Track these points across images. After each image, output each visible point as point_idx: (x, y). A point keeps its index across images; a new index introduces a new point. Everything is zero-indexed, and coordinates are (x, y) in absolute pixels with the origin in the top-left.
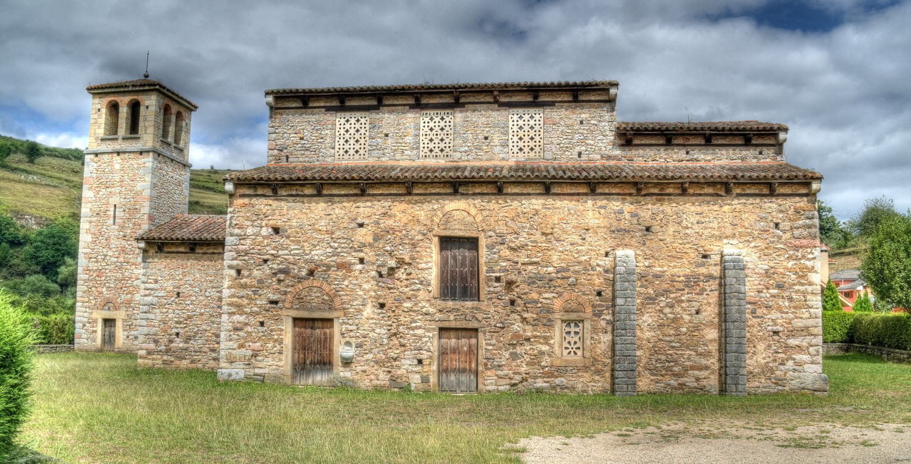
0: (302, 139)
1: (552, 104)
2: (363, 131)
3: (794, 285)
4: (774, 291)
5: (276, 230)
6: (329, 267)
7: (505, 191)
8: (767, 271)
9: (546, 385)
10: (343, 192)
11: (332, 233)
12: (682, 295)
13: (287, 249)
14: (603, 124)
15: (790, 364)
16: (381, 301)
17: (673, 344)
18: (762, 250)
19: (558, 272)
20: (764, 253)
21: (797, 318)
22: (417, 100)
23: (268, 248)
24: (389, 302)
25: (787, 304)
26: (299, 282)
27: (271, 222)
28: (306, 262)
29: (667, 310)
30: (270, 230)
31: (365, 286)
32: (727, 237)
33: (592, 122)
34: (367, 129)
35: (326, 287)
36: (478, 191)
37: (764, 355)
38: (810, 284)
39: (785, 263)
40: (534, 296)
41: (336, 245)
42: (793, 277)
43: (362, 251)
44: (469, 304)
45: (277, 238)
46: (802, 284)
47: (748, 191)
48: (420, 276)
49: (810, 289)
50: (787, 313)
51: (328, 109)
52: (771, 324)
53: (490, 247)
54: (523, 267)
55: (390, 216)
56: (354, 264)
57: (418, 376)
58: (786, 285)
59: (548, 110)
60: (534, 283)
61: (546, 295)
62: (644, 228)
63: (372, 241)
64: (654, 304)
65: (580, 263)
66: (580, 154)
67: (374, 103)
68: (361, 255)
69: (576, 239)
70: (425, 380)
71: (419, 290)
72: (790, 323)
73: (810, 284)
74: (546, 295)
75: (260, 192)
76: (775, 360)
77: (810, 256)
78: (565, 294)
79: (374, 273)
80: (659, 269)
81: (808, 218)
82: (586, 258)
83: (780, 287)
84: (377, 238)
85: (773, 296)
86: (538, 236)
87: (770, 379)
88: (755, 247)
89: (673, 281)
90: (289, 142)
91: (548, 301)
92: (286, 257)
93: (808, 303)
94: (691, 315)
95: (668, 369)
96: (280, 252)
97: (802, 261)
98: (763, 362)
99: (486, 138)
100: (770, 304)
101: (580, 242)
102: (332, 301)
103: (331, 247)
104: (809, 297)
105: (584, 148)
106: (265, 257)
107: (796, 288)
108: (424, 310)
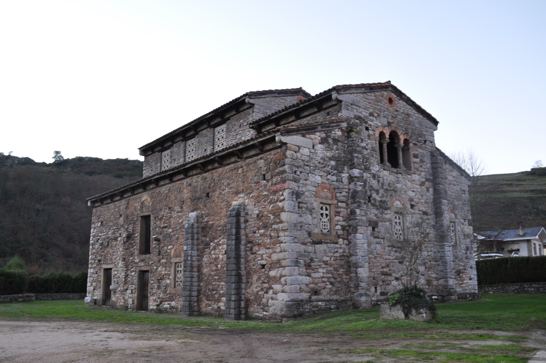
1: (229, 119)
3: (273, 224)
4: (262, 231)
12: (220, 241)
15: (271, 292)
20: (258, 200)
21: (275, 252)
22: (184, 137)
25: (269, 241)
38: (281, 222)
42: (272, 217)
49: (281, 225)
69: (179, 210)
72: (270, 257)
73: (281, 222)
76: (262, 289)
77: (282, 198)
80: (211, 223)
81: (281, 166)
83: (265, 227)
88: (252, 197)
89: (217, 230)
94: (222, 254)
100: (260, 242)
104: (281, 234)
107: (273, 226)
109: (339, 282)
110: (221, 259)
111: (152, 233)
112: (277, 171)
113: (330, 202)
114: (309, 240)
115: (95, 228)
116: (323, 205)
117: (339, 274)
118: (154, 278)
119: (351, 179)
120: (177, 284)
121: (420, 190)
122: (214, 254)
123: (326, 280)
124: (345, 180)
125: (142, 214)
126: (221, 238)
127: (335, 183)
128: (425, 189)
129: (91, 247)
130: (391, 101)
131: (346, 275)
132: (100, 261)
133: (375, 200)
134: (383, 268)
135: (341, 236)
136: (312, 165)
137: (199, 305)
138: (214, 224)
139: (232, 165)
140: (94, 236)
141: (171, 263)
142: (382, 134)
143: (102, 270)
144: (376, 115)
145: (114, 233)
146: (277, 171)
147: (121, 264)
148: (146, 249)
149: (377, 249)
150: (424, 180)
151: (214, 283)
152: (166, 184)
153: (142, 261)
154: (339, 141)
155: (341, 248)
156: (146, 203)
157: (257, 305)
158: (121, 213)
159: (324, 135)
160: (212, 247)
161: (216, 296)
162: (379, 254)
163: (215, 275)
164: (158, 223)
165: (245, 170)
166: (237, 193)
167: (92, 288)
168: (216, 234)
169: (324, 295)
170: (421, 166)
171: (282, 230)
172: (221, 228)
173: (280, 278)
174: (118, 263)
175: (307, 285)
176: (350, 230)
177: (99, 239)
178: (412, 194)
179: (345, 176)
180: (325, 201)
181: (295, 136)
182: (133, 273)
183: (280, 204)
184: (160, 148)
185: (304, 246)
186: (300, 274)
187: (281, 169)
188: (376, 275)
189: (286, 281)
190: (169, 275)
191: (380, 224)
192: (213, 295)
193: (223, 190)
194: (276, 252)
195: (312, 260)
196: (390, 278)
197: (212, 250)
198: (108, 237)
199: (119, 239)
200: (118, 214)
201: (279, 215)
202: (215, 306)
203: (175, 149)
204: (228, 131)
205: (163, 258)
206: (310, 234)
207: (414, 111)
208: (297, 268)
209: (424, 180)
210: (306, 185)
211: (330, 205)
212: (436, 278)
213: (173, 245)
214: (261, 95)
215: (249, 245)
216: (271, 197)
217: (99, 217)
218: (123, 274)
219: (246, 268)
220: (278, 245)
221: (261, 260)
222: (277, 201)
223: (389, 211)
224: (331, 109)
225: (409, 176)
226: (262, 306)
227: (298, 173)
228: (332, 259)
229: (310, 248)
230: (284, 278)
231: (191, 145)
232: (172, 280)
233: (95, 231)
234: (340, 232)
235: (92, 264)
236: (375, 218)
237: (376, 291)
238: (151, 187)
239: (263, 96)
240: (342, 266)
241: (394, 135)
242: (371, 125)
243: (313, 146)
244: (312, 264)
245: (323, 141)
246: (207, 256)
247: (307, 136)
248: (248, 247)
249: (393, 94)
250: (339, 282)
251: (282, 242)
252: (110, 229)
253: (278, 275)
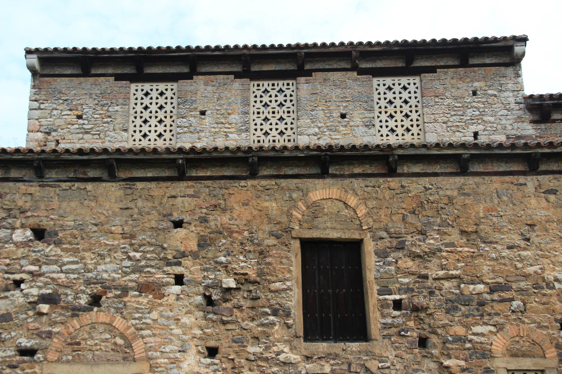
0: (80, 117)
1: (432, 70)
2: (168, 108)
5: (40, 234)
6: (125, 290)
7: (399, 171)
10: (149, 175)
11: (132, 237)
13: (56, 262)
14: (506, 94)
16: (212, 344)
19: (492, 291)
23: (23, 262)
24: (224, 346)
26: (73, 316)
27: (31, 221)
28: (88, 282)
30: (29, 233)
31: (185, 320)
33: (490, 92)
34: (175, 104)
35: (119, 322)
36: (357, 170)
40: (460, 330)
41: (138, 255)
43: (179, 264)
44: (355, 346)
45: (40, 246)
48: (273, 302)
51: (119, 77)
53: (382, 254)
54: (437, 284)
55: (224, 210)
56: (168, 284)
59: (428, 76)
60: (456, 309)
61: (478, 329)
63: (195, 248)
65: (526, 276)
66: (476, 135)
67: (186, 70)
68: (178, 270)
71: (273, 324)
74: (478, 329)
75: (14, 174)
78: (508, 327)
79: (199, 299)
82: (536, 268)
84: (203, 243)
86: (455, 236)
90: (59, 122)
91: (483, 339)
92: (55, 275)
96: (45, 268)
99: (343, 116)
101: (523, 244)
102: (130, 346)
103: (129, 258)
106: (18, 277)
108: (282, 357)
152: (436, 175)
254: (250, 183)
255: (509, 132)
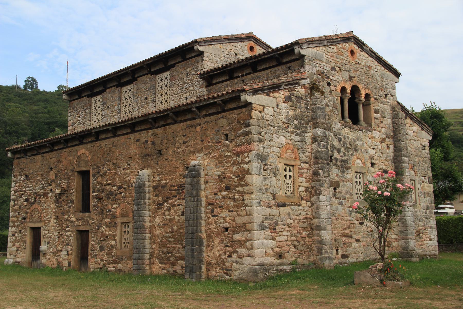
1: (173, 66)
3: (237, 186)
4: (224, 193)
8: (219, 176)
9: (113, 269)
12: (175, 201)
15: (235, 256)
17: (170, 239)
18: (217, 159)
20: (219, 161)
21: (239, 215)
25: (232, 203)
29: (167, 213)
32: (198, 152)
37: (218, 248)
39: (231, 169)
42: (236, 179)
46: (242, 186)
47: (210, 112)
50: (232, 211)
52: (222, 221)
53: (94, 176)
57: (67, 262)
58: (232, 187)
62: (157, 152)
64: (160, 208)
70: (69, 264)
72: (234, 221)
76: (225, 253)
77: (247, 160)
83: (228, 188)
85: (223, 197)
86: (111, 166)
87: (223, 269)
88: (213, 157)
89: (171, 190)
93: (245, 201)
94: (178, 216)
95: (168, 259)
97: (242, 166)
98: (218, 254)
100: (222, 204)
105: (188, 94)
107: (237, 189)
109: (303, 245)
110: (176, 221)
111: (91, 190)
112: (241, 131)
113: (293, 163)
114: (273, 202)
115: (16, 182)
116: (286, 166)
117: (302, 237)
118: (95, 239)
119: (314, 139)
120: (123, 245)
121: (380, 148)
122: (169, 215)
123: (290, 243)
124: (308, 140)
125: (79, 169)
126: (177, 198)
127: (298, 143)
128: (386, 146)
129: (12, 203)
130: (352, 53)
131: (309, 237)
132: (24, 218)
133: (336, 159)
134: (344, 229)
135: (304, 198)
136: (276, 125)
137: (151, 268)
138: (168, 183)
139: (188, 123)
140: (16, 191)
141: (116, 223)
142: (343, 89)
143: (28, 229)
144: (337, 69)
145: (43, 188)
146: (241, 131)
147: (53, 222)
148: (86, 208)
149: (339, 210)
150: (384, 136)
151: (169, 245)
152: (108, 138)
153: (78, 220)
154: (302, 99)
155: (304, 210)
156: (83, 157)
157: (220, 269)
158: (52, 166)
159: (288, 94)
160: (165, 208)
161: (171, 259)
162: (340, 215)
163: (170, 237)
164: (100, 179)
165: (204, 128)
166: (193, 153)
167: (15, 249)
168: (171, 194)
169: (289, 258)
170: (382, 122)
171: (248, 193)
172: (176, 187)
173: (245, 242)
174: (49, 222)
175: (272, 249)
176: (313, 192)
177: (22, 194)
178: (372, 152)
179: (308, 135)
180: (288, 163)
181: (260, 96)
182: (69, 233)
183: (245, 166)
184: (89, 93)
185: (269, 210)
186: (265, 238)
187: (246, 130)
188: (337, 237)
189: (252, 246)
190: (114, 236)
191: (341, 184)
192: (168, 259)
193: (178, 148)
194: (241, 216)
195: (277, 224)
196: (350, 240)
197: (166, 210)
198: (35, 193)
199: (50, 195)
200: (47, 167)
201: (244, 177)
202: (170, 269)
203: (108, 94)
204: (173, 79)
205: (106, 218)
206: (274, 197)
207: (376, 63)
208: (262, 231)
209: (384, 136)
210: (270, 146)
211: (293, 166)
212: (396, 239)
213: (119, 204)
214: (211, 42)
215: (210, 207)
216: (235, 158)
217: (22, 169)
218: (56, 234)
219: (206, 231)
220: (242, 208)
221: (223, 223)
222: (240, 163)
223: (349, 170)
224: (292, 64)
225: (370, 133)
226: (225, 271)
227: (263, 134)
228: (296, 221)
229: (275, 211)
230: (250, 242)
231: (128, 91)
232: (118, 241)
233: (18, 185)
234: (303, 194)
235: (14, 222)
236: (336, 178)
237: (337, 254)
238: (90, 140)
239: (213, 43)
240: (305, 229)
241: (355, 89)
242: (333, 80)
243: (277, 105)
244: (277, 227)
245: (287, 99)
246: (160, 217)
247: (271, 95)
248: (209, 209)
249: (355, 46)
250: (303, 245)
251: (247, 206)
252: (37, 184)
253: (243, 239)
254: (66, 150)
255: (197, 95)
